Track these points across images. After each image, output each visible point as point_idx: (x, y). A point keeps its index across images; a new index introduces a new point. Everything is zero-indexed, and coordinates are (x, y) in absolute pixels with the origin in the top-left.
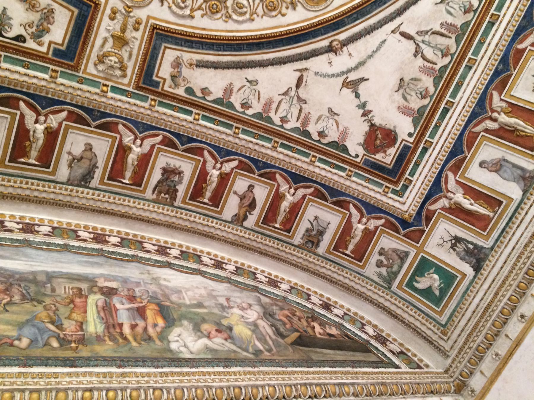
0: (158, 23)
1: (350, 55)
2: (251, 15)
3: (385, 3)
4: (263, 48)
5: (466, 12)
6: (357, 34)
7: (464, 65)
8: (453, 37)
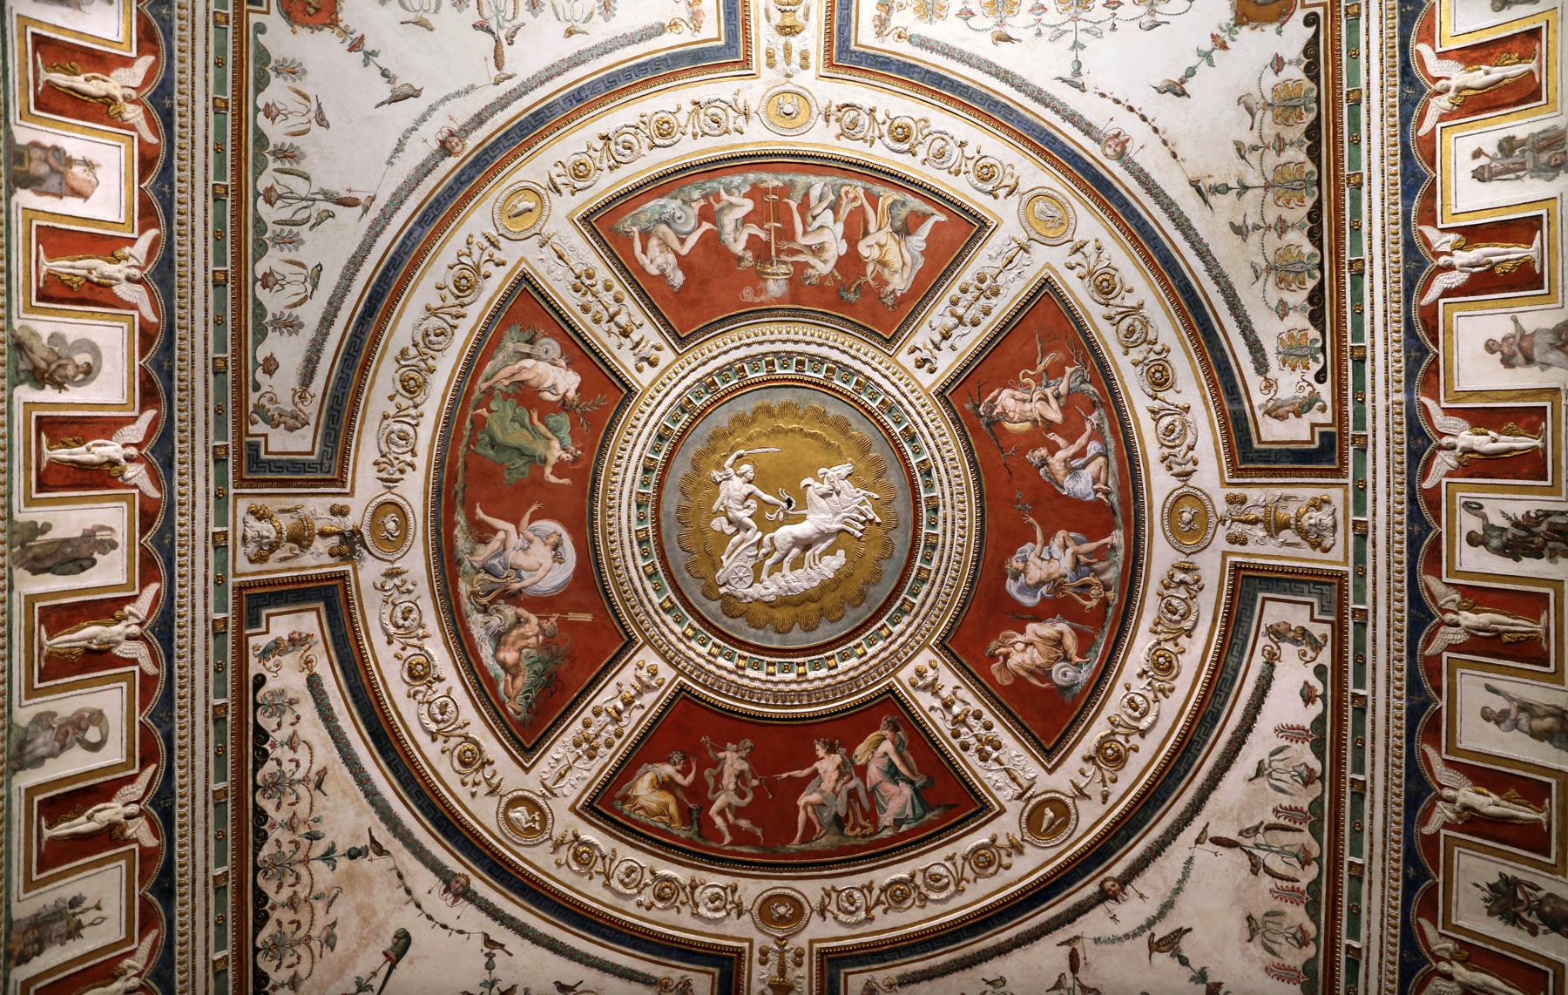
0: (825, 945)
1: (1141, 896)
2: (957, 885)
3: (1164, 801)
4: (994, 926)
5: (1306, 783)
6: (1138, 860)
7: (1346, 876)
8: (1305, 827)
